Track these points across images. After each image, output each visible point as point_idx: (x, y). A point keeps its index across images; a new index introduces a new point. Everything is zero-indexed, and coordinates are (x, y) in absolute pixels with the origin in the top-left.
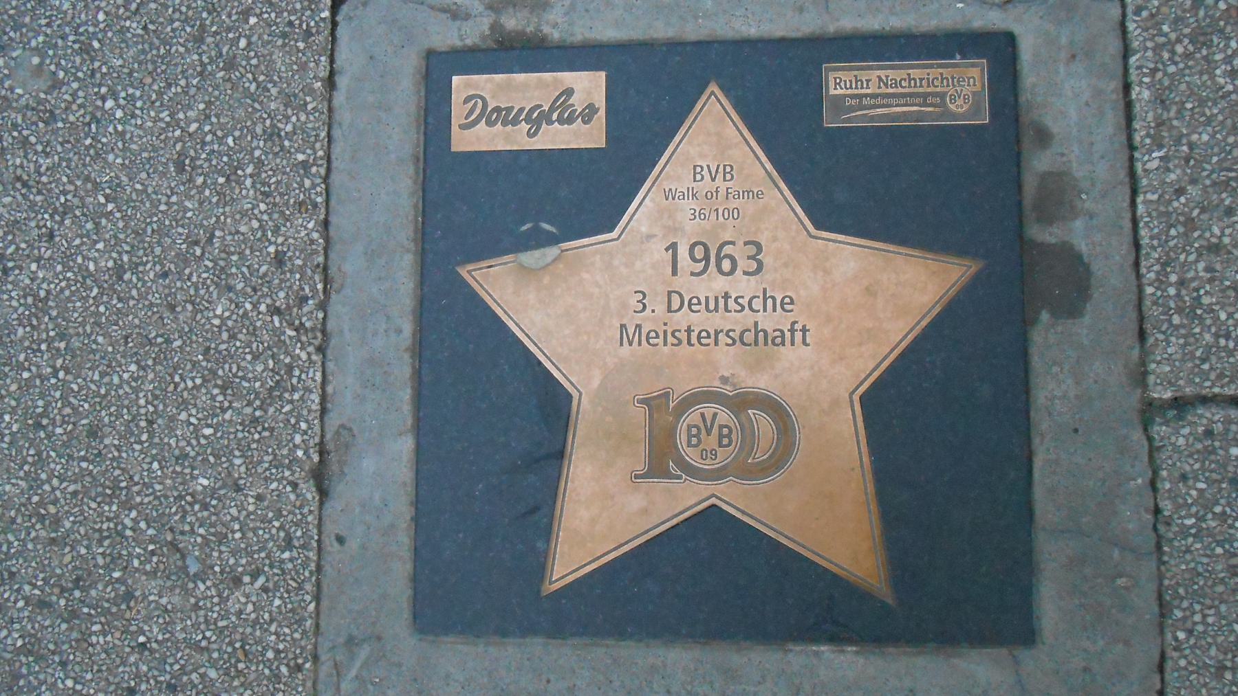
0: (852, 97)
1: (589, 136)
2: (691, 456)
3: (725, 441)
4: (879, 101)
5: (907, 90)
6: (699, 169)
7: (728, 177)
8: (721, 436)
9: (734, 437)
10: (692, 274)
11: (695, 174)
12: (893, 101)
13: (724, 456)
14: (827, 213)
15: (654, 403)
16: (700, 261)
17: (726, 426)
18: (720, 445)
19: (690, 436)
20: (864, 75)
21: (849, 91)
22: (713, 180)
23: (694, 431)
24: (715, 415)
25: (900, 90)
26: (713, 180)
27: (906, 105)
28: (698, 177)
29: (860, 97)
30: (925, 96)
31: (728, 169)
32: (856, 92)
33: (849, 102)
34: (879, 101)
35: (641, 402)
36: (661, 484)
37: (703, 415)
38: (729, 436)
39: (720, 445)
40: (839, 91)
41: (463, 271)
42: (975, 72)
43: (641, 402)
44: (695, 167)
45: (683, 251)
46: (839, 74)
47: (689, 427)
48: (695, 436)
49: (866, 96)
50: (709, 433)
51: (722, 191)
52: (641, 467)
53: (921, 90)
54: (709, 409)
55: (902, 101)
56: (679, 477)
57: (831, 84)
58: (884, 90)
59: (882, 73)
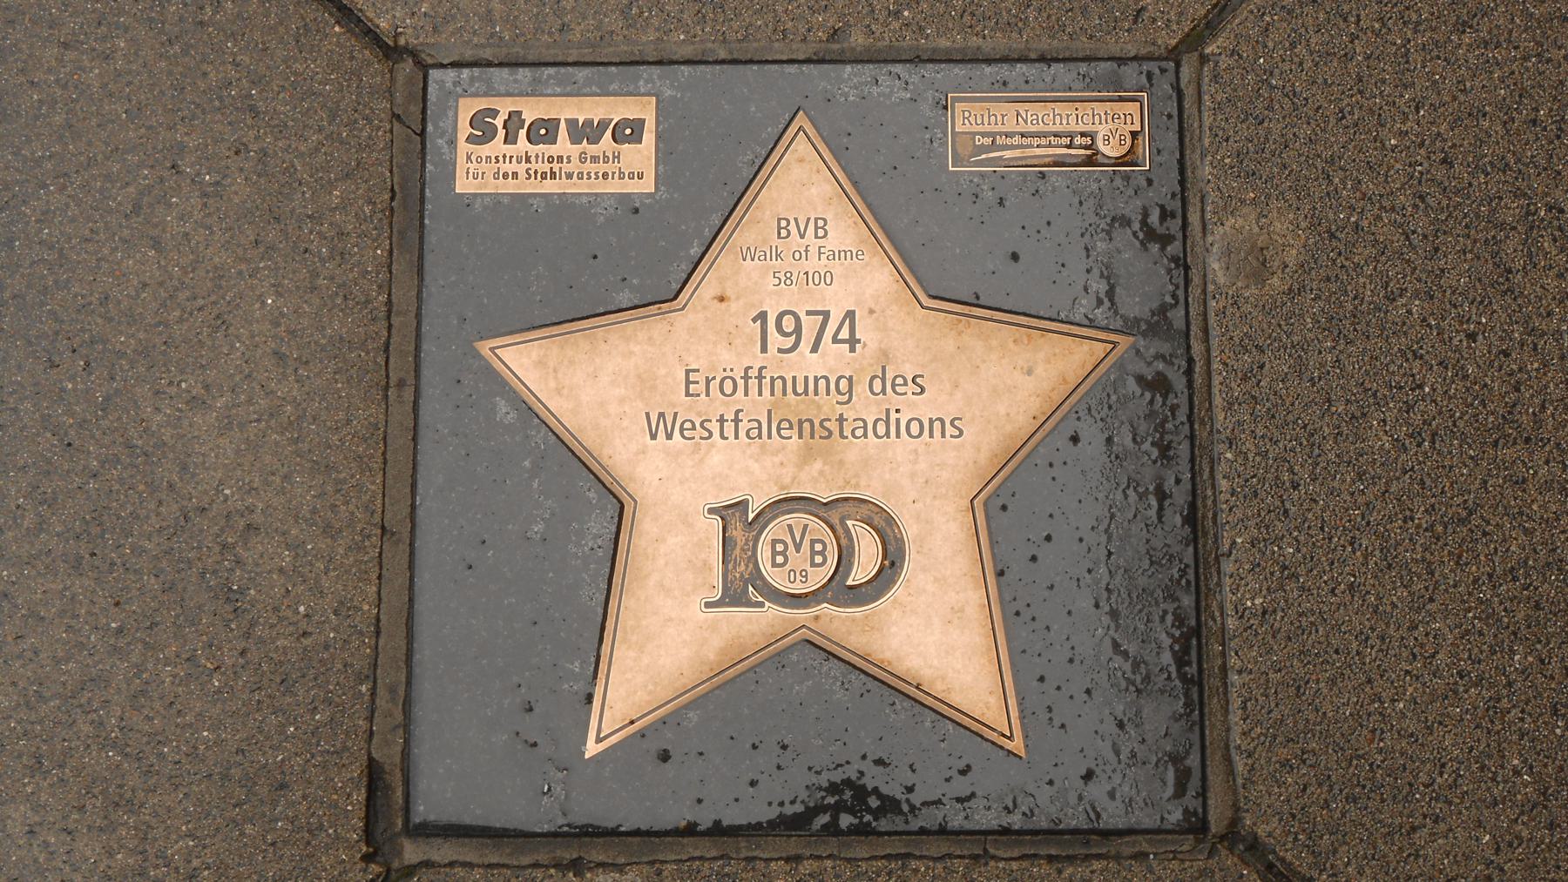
0: (984, 135)
2: (777, 579)
3: (818, 559)
4: (1016, 140)
6: (783, 223)
7: (821, 233)
8: (813, 553)
10: (780, 351)
11: (779, 228)
12: (1036, 141)
15: (731, 512)
18: (813, 564)
19: (774, 553)
21: (980, 129)
22: (802, 237)
23: (780, 548)
24: (806, 526)
25: (1041, 128)
26: (802, 237)
27: (1050, 146)
28: (784, 233)
29: (993, 135)
30: (1071, 136)
31: (821, 223)
32: (987, 128)
33: (979, 140)
34: (1016, 140)
35: (711, 511)
36: (739, 613)
37: (790, 526)
38: (822, 553)
39: (813, 564)
40: (967, 128)
41: (484, 347)
43: (711, 511)
44: (779, 220)
47: (774, 542)
49: (1001, 134)
50: (798, 548)
54: (797, 519)
55: (1044, 141)
56: (761, 605)
57: (959, 122)
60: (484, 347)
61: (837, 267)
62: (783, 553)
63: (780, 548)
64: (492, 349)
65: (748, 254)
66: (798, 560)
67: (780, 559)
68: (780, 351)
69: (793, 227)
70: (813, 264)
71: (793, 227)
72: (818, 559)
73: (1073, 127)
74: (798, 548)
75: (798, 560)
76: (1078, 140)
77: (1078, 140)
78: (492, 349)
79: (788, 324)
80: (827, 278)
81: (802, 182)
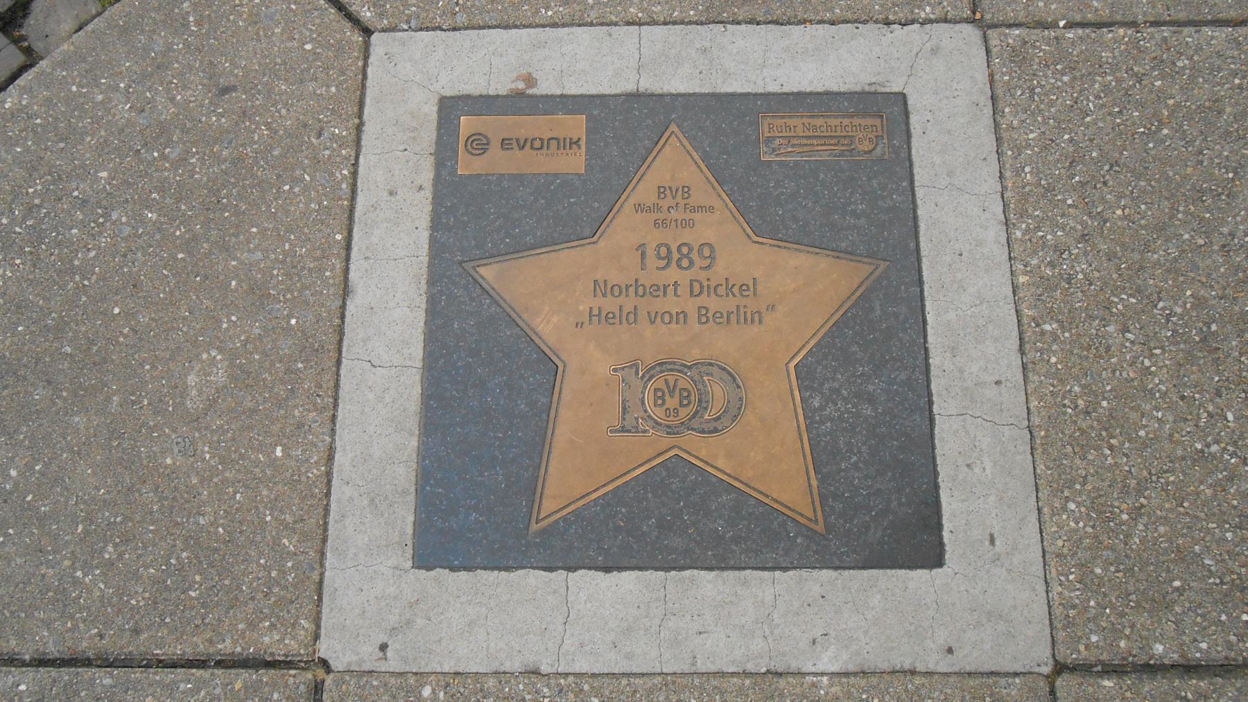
1: (574, 163)
4: (805, 141)
9: (693, 398)
10: (658, 268)
11: (659, 193)
14: (768, 220)
16: (663, 259)
17: (689, 392)
18: (681, 405)
20: (792, 122)
22: (674, 198)
26: (674, 198)
34: (805, 141)
45: (650, 252)
48: (659, 398)
50: (672, 392)
51: (681, 206)
58: (807, 133)
59: (806, 121)
61: (692, 216)
62: (662, 398)
63: (659, 394)
64: (474, 268)
65: (639, 207)
66: (672, 402)
67: (660, 402)
68: (658, 268)
69: (668, 192)
71: (668, 192)
74: (672, 392)
75: (672, 402)
78: (474, 268)
80: (689, 224)
81: (674, 162)
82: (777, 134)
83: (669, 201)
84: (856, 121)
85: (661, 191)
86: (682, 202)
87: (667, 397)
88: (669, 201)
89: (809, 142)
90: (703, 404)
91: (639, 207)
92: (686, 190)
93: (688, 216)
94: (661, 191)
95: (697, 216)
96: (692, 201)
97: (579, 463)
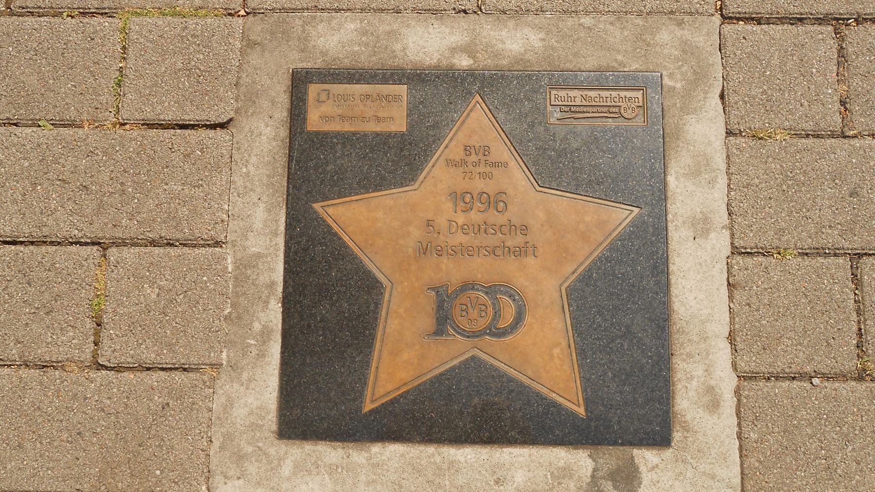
4: (581, 109)
5: (598, 104)
9: (488, 312)
12: (589, 109)
13: (483, 323)
21: (565, 103)
34: (581, 109)
35: (433, 289)
42: (639, 94)
46: (556, 92)
51: (483, 162)
52: (433, 328)
53: (605, 104)
55: (595, 110)
57: (553, 97)
58: (584, 103)
60: (317, 206)
65: (449, 162)
69: (473, 151)
70: (481, 169)
71: (473, 151)
72: (483, 314)
73: (609, 104)
75: (474, 313)
76: (612, 110)
77: (612, 110)
79: (468, 198)
82: (560, 103)
83: (473, 158)
84: (623, 94)
85: (467, 149)
86: (483, 158)
87: (471, 311)
88: (473, 158)
89: (585, 109)
90: (497, 315)
91: (449, 162)
92: (486, 151)
93: (488, 169)
94: (467, 149)
95: (495, 171)
96: (491, 159)
97: (402, 357)
